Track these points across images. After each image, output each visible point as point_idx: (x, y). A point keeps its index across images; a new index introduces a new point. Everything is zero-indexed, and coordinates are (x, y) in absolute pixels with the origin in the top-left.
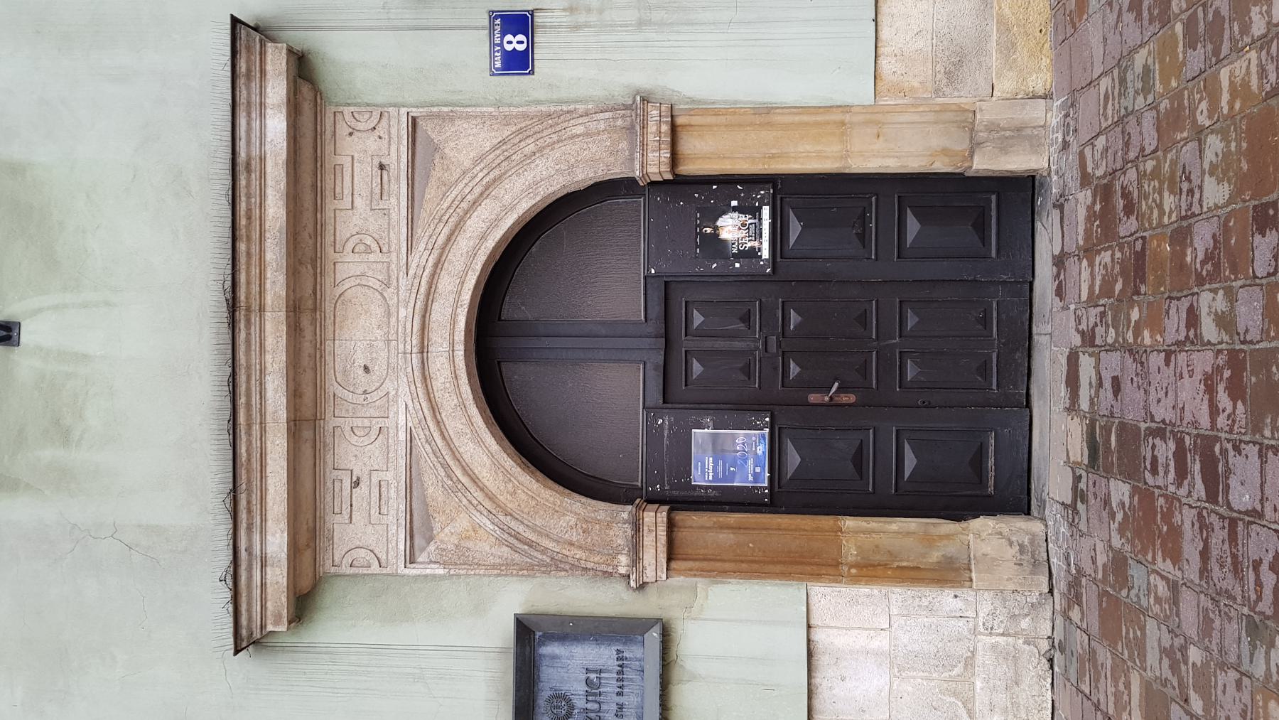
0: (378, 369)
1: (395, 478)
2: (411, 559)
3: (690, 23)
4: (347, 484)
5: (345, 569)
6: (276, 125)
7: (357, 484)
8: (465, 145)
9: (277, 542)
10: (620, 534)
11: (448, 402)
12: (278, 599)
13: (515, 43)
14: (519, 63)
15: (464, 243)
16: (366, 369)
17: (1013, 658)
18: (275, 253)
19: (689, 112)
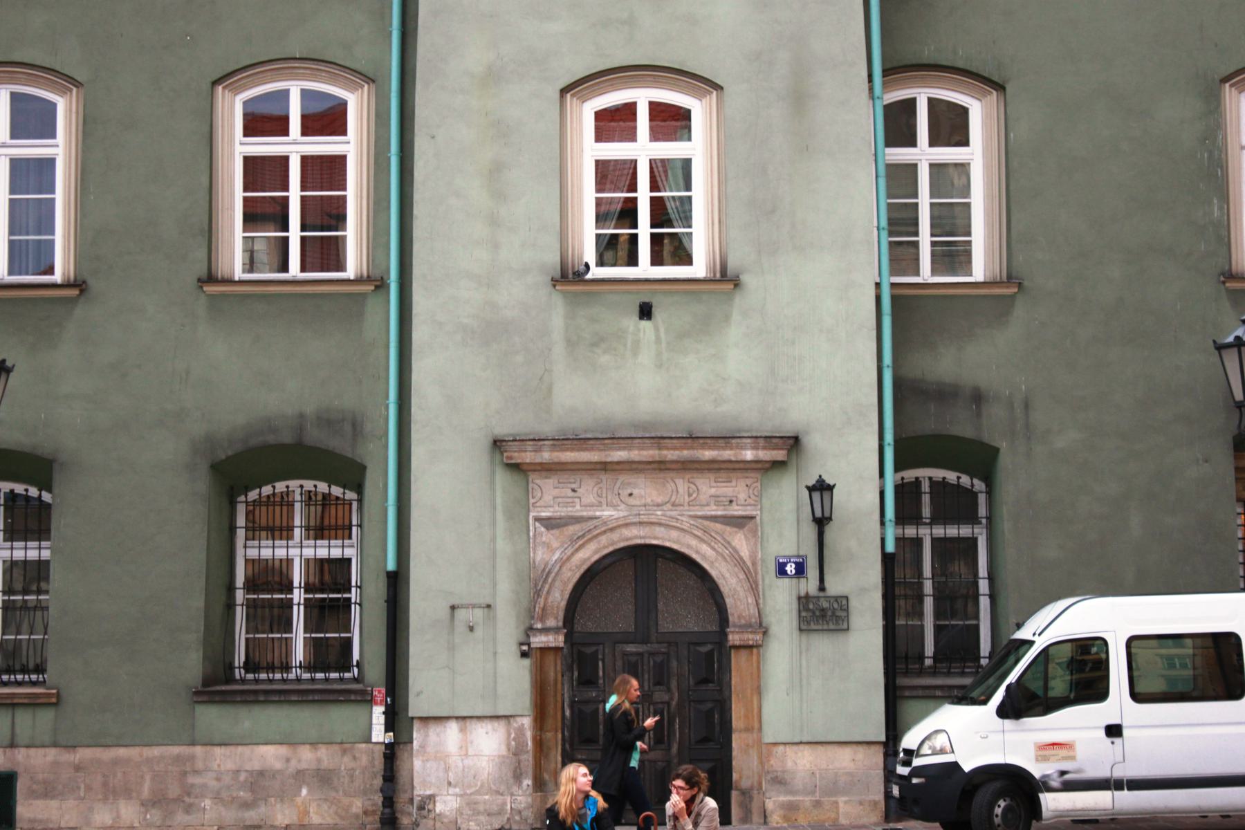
0: (631, 501)
1: (577, 510)
2: (537, 519)
3: (801, 653)
4: (573, 486)
5: (531, 485)
6: (749, 455)
7: (574, 490)
8: (740, 541)
9: (546, 456)
10: (551, 623)
11: (615, 536)
12: (518, 458)
13: (790, 569)
14: (781, 571)
15: (694, 542)
16: (631, 495)
17: (500, 812)
18: (686, 454)
19: (759, 654)
